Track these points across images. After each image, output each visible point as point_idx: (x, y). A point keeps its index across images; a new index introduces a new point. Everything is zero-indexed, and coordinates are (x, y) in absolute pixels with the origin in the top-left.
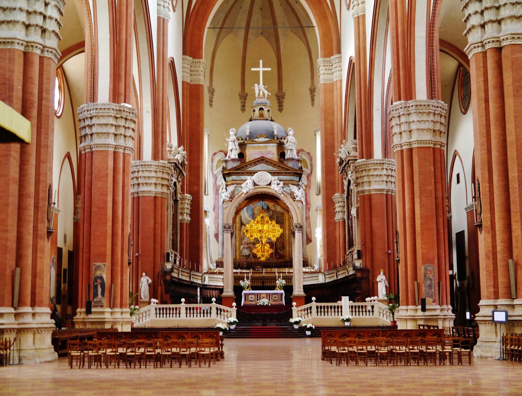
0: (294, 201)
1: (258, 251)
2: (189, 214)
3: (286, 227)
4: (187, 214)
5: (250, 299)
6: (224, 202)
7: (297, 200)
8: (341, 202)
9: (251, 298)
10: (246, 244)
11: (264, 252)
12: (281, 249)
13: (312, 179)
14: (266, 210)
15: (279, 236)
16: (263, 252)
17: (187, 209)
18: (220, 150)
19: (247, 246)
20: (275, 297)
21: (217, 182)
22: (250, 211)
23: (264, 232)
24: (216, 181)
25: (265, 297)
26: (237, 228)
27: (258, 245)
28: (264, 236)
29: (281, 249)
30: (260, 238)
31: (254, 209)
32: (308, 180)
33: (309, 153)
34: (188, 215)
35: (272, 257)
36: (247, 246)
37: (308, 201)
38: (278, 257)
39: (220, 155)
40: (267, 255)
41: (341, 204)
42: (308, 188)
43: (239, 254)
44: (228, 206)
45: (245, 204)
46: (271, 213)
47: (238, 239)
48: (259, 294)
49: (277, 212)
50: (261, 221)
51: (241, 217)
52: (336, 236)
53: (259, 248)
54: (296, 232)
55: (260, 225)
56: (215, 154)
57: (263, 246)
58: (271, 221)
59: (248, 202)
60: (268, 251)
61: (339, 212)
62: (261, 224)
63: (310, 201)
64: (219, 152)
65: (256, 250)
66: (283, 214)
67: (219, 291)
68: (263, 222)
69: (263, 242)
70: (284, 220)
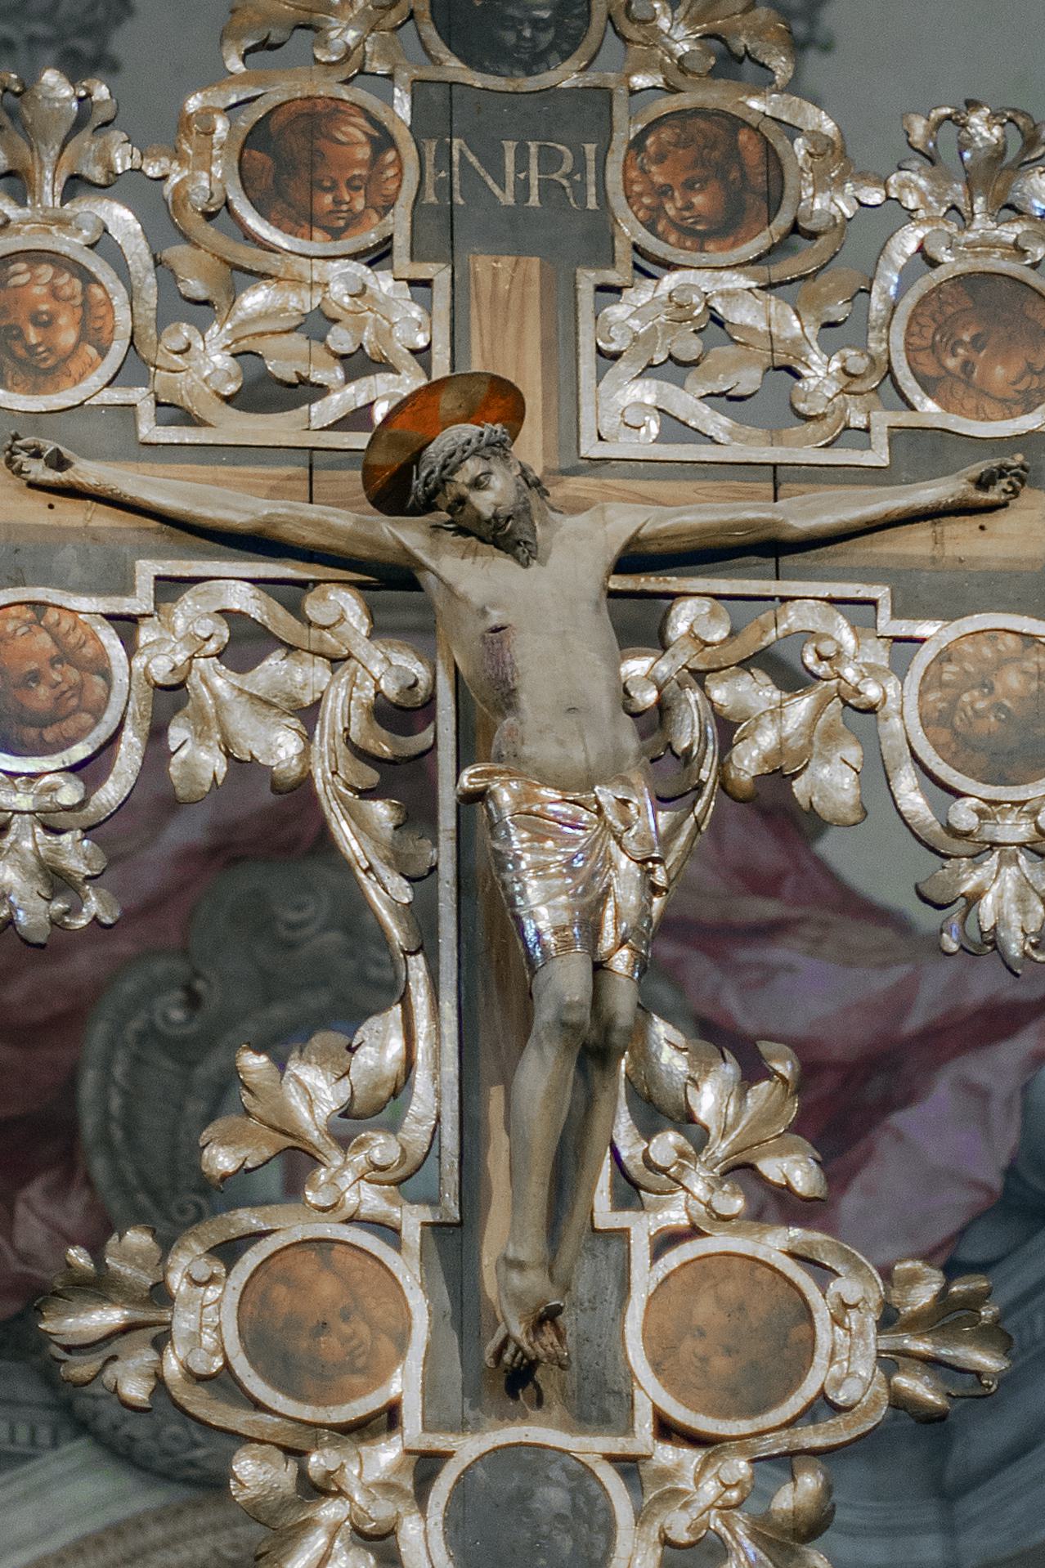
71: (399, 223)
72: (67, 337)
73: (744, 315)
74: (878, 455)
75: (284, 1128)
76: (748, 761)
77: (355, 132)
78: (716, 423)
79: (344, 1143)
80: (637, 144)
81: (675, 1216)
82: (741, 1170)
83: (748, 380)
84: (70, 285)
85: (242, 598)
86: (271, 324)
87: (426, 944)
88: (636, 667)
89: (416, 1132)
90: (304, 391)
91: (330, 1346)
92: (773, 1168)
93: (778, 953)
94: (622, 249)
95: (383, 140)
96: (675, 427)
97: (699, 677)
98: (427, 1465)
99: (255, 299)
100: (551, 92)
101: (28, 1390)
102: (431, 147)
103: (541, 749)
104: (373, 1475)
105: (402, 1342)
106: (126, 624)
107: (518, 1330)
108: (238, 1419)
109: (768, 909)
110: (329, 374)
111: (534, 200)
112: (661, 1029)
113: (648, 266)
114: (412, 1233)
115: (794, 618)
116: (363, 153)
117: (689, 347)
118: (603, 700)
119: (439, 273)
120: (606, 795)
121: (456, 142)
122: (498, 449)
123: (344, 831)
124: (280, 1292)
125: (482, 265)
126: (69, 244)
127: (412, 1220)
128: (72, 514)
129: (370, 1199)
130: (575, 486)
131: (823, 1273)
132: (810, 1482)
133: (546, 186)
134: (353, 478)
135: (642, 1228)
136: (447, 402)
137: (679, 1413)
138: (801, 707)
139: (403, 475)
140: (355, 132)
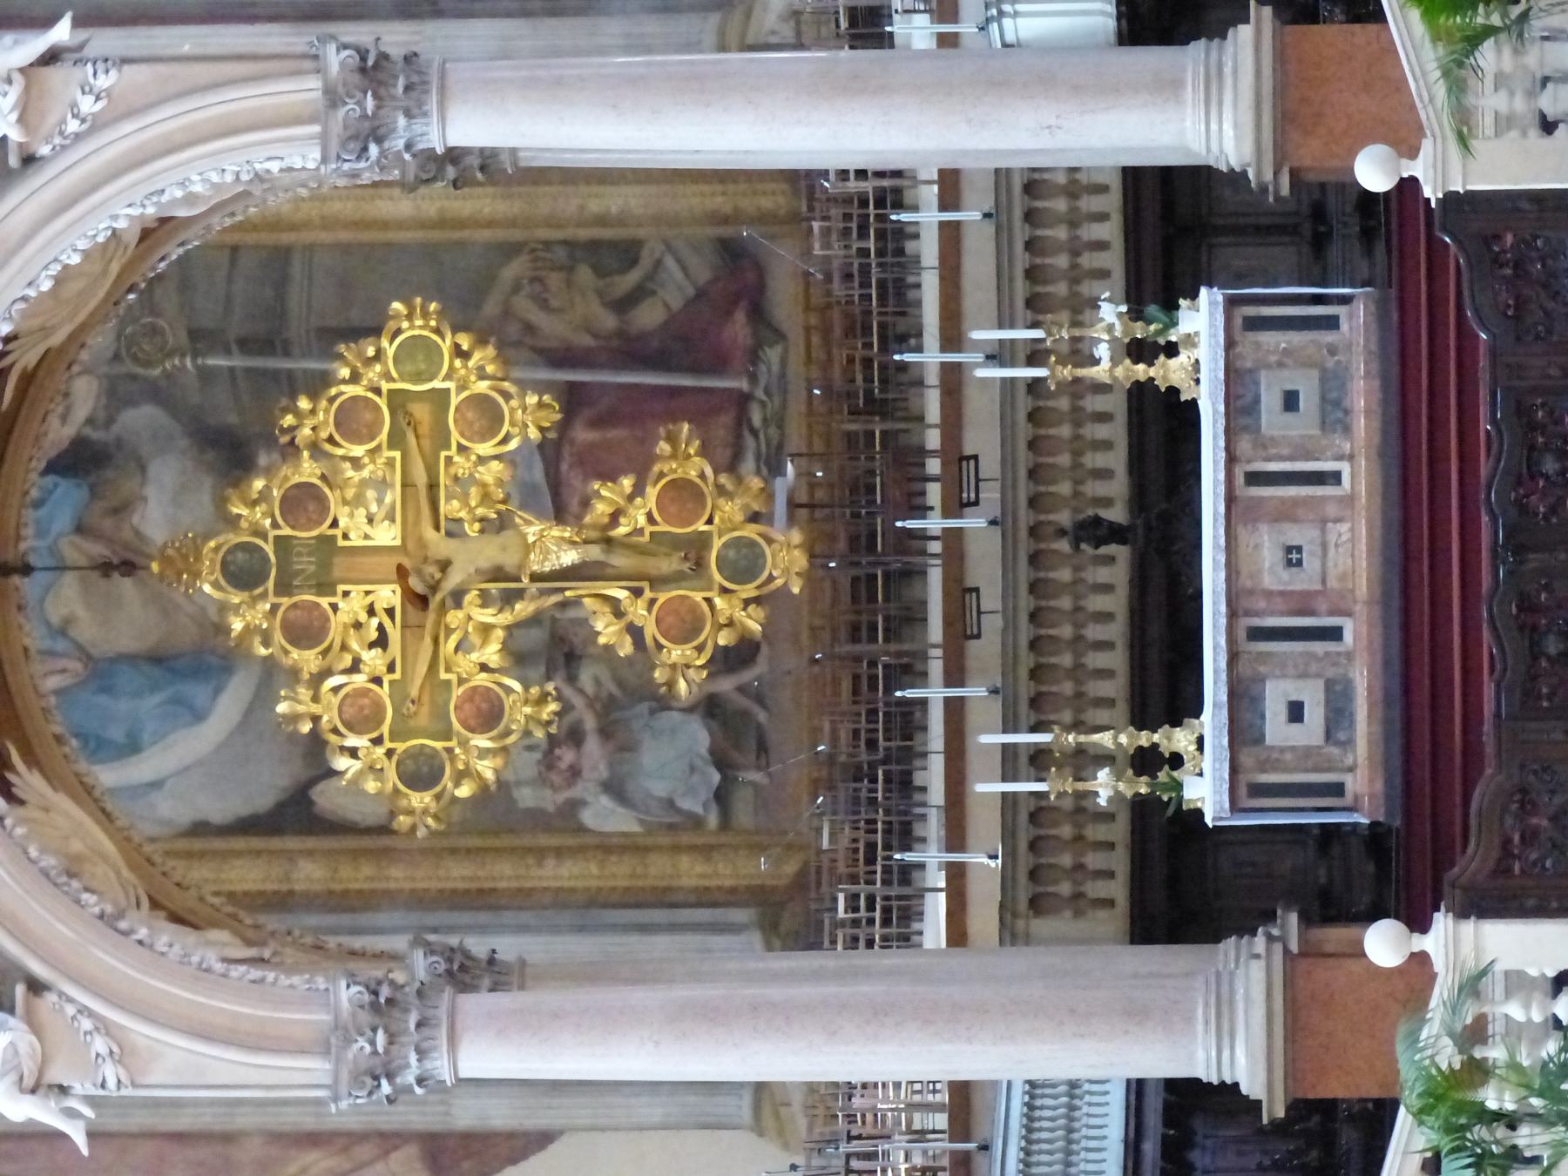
0: (29, 160)
1: (686, 627)
5: (1311, 730)
6: (55, 1075)
7: (21, 120)
9: (1296, 712)
10: (567, 756)
11: (703, 541)
12: (628, 281)
14: (94, 493)
15: (483, 356)
16: (700, 565)
19: (592, 745)
20: (1291, 401)
22: (123, 706)
25: (1295, 534)
26: (359, 876)
27: (607, 630)
28: (491, 552)
29: (628, 281)
30: (509, 598)
35: (743, 400)
36: (592, 745)
38: (739, 328)
40: (731, 509)
43: (706, 851)
44: (104, 1027)
45: (62, 801)
46: (141, 419)
47: (504, 873)
48: (1232, 615)
50: (283, 588)
51: (201, 829)
53: (638, 612)
54: (433, 141)
55: (352, 606)
57: (620, 561)
58: (291, 450)
59: (32, 760)
60: (683, 495)
62: (326, 588)
65: (676, 653)
67: (1199, 1124)
68: (306, 564)
69: (569, 557)
70: (235, 249)
71: (324, 602)
72: (366, 701)
74: (397, 454)
75: (620, 631)
80: (293, 528)
82: (630, 498)
84: (349, 701)
86: (361, 641)
87: (563, 590)
88: (472, 529)
89: (622, 594)
90: (381, 628)
91: (688, 618)
94: (331, 532)
95: (294, 606)
97: (471, 510)
98: (724, 591)
99: (355, 646)
100: (275, 552)
102: (296, 591)
104: (726, 606)
105: (687, 597)
106: (461, 681)
107: (688, 565)
108: (710, 645)
110: (374, 622)
111: (313, 559)
116: (299, 612)
117: (362, 512)
119: (341, 588)
120: (531, 539)
121: (295, 583)
124: (673, 632)
126: (335, 701)
128: (426, 698)
133: (309, 554)
137: (706, 517)
140: (292, 615)
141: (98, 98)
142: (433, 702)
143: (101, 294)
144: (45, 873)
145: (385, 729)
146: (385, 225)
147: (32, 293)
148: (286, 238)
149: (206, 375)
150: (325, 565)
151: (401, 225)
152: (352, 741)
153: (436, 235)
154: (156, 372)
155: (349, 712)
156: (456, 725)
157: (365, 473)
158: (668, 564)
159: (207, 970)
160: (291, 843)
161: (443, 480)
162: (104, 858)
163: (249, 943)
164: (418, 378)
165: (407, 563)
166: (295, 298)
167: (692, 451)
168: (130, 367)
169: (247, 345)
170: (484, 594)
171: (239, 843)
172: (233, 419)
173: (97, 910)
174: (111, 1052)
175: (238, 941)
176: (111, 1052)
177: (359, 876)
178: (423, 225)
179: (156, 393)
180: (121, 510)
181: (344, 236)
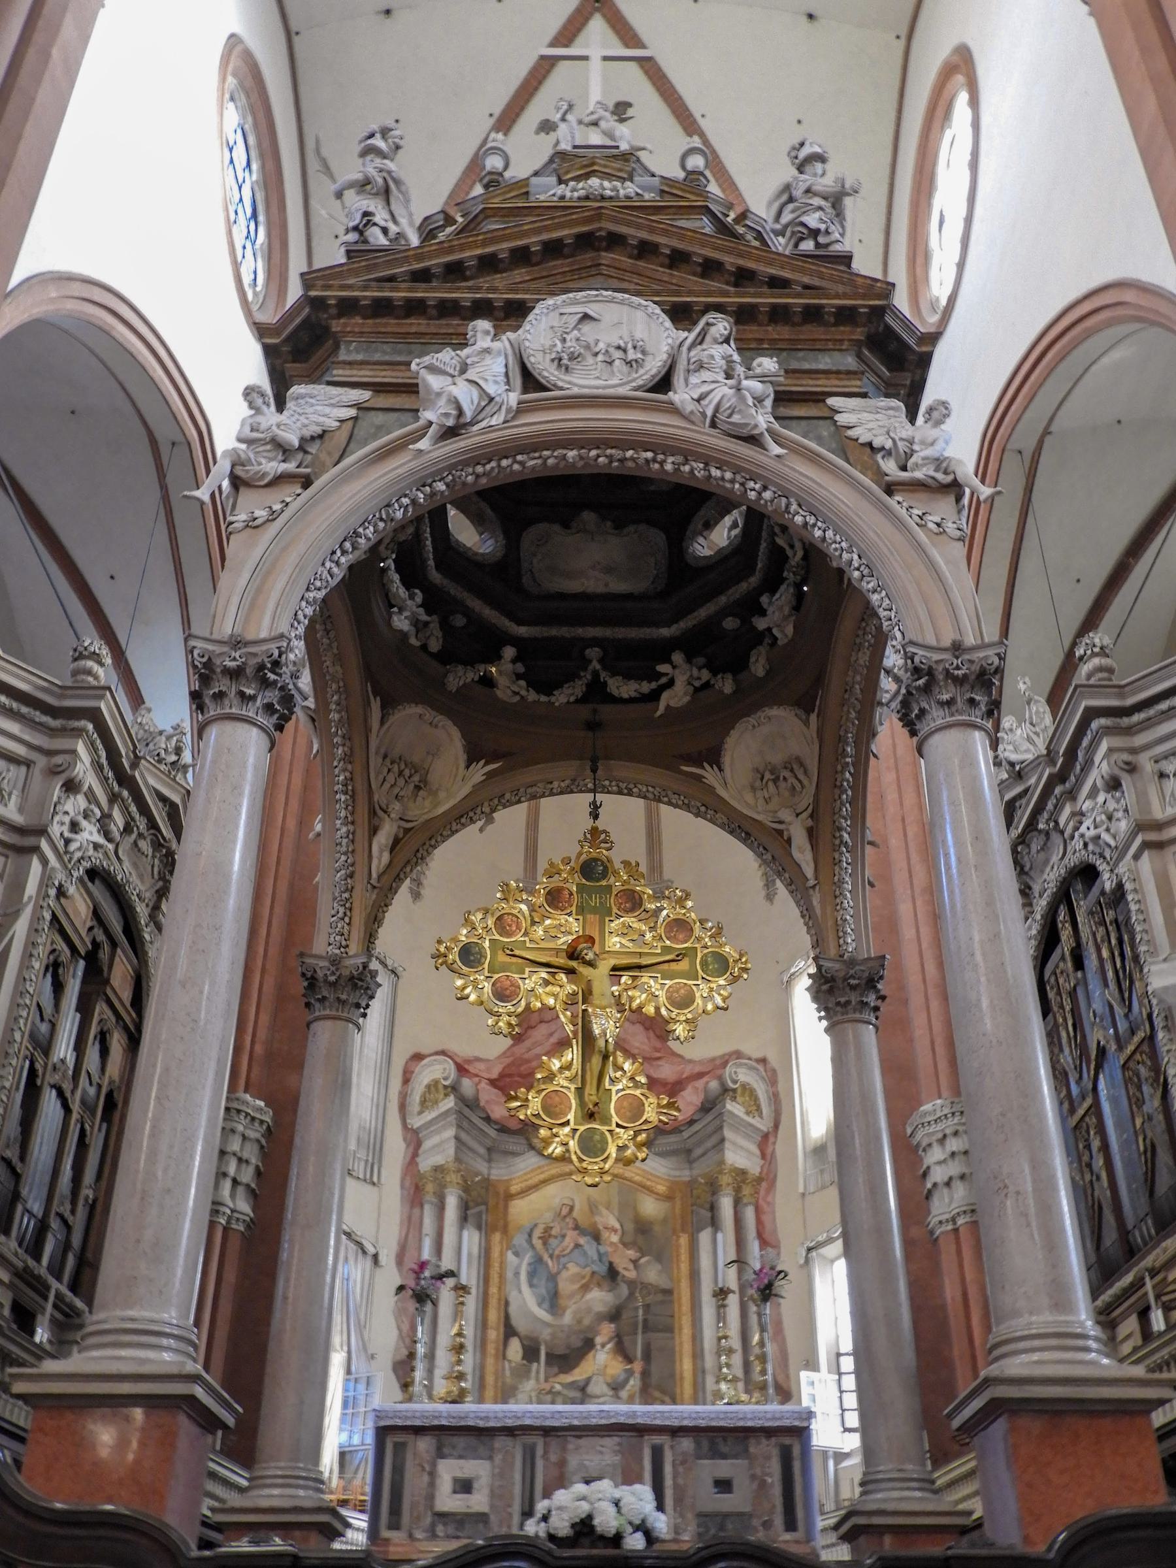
2: (248, 1186)
3: (681, 1343)
4: (235, 1182)
8: (956, 1133)
13: (780, 1148)
17: (240, 1160)
18: (440, 1048)
21: (418, 1160)
22: (543, 1282)
23: (605, 966)
24: (415, 1155)
26: (491, 1349)
31: (559, 1273)
32: (763, 1156)
33: (763, 1061)
34: (240, 1190)
37: (766, 1236)
39: (438, 1067)
40: (624, 1136)
41: (953, 1145)
42: (764, 1184)
44: (273, 516)
45: (466, 790)
46: (624, 1290)
49: (646, 1287)
51: (507, 1303)
52: (943, 1307)
53: (561, 1081)
56: (418, 1057)
59: (490, 775)
61: (948, 1184)
62: (581, 910)
63: (775, 1231)
64: (437, 1053)
66: (668, 1292)
68: (595, 901)
70: (672, 1316)
71: (574, 909)
73: (634, 925)
76: (635, 1005)
77: (566, 892)
78: (630, 945)
79: (561, 1073)
81: (620, 1086)
82: (632, 1079)
83: (635, 937)
85: (544, 975)
88: (614, 988)
89: (573, 1071)
92: (638, 1078)
93: (660, 1063)
95: (571, 894)
96: (622, 945)
99: (548, 922)
101: (523, 1141)
103: (596, 1002)
109: (658, 1055)
112: (618, 1053)
113: (619, 917)
114: (573, 1089)
115: (644, 980)
118: (609, 994)
119: (580, 917)
122: (590, 948)
123: (561, 1016)
125: (588, 916)
126: (515, 912)
127: (573, 1087)
128: (514, 960)
129: (566, 1083)
130: (605, 956)
131: (647, 1098)
132: (644, 1135)
134: (564, 954)
135: (614, 1089)
136: (582, 940)
138: (644, 996)
139: (573, 953)
141: (938, 525)
142: (513, 963)
143: (745, 811)
144: (388, 505)
145: (497, 937)
146: (681, 1360)
147: (794, 507)
148: (676, 1331)
149: (637, 1308)
150: (594, 910)
151: (681, 1366)
152: (490, 922)
153: (678, 1377)
154: (637, 1294)
155: (508, 919)
156: (496, 976)
157: (648, 936)
158: (591, 1090)
159: (308, 589)
160: (502, 1330)
161: (645, 978)
162: (435, 806)
163: (380, 877)
164: (704, 964)
165: (597, 948)
166: (661, 1335)
167: (663, 1118)
168: (639, 1287)
169: (645, 1321)
170: (575, 994)
171: (502, 1315)
172: (624, 1316)
173: (361, 530)
174: (255, 519)
175: (381, 870)
176: (255, 519)
177: (491, 1349)
178: (681, 1374)
179: (631, 1295)
180: (599, 1285)
181: (677, 1349)
